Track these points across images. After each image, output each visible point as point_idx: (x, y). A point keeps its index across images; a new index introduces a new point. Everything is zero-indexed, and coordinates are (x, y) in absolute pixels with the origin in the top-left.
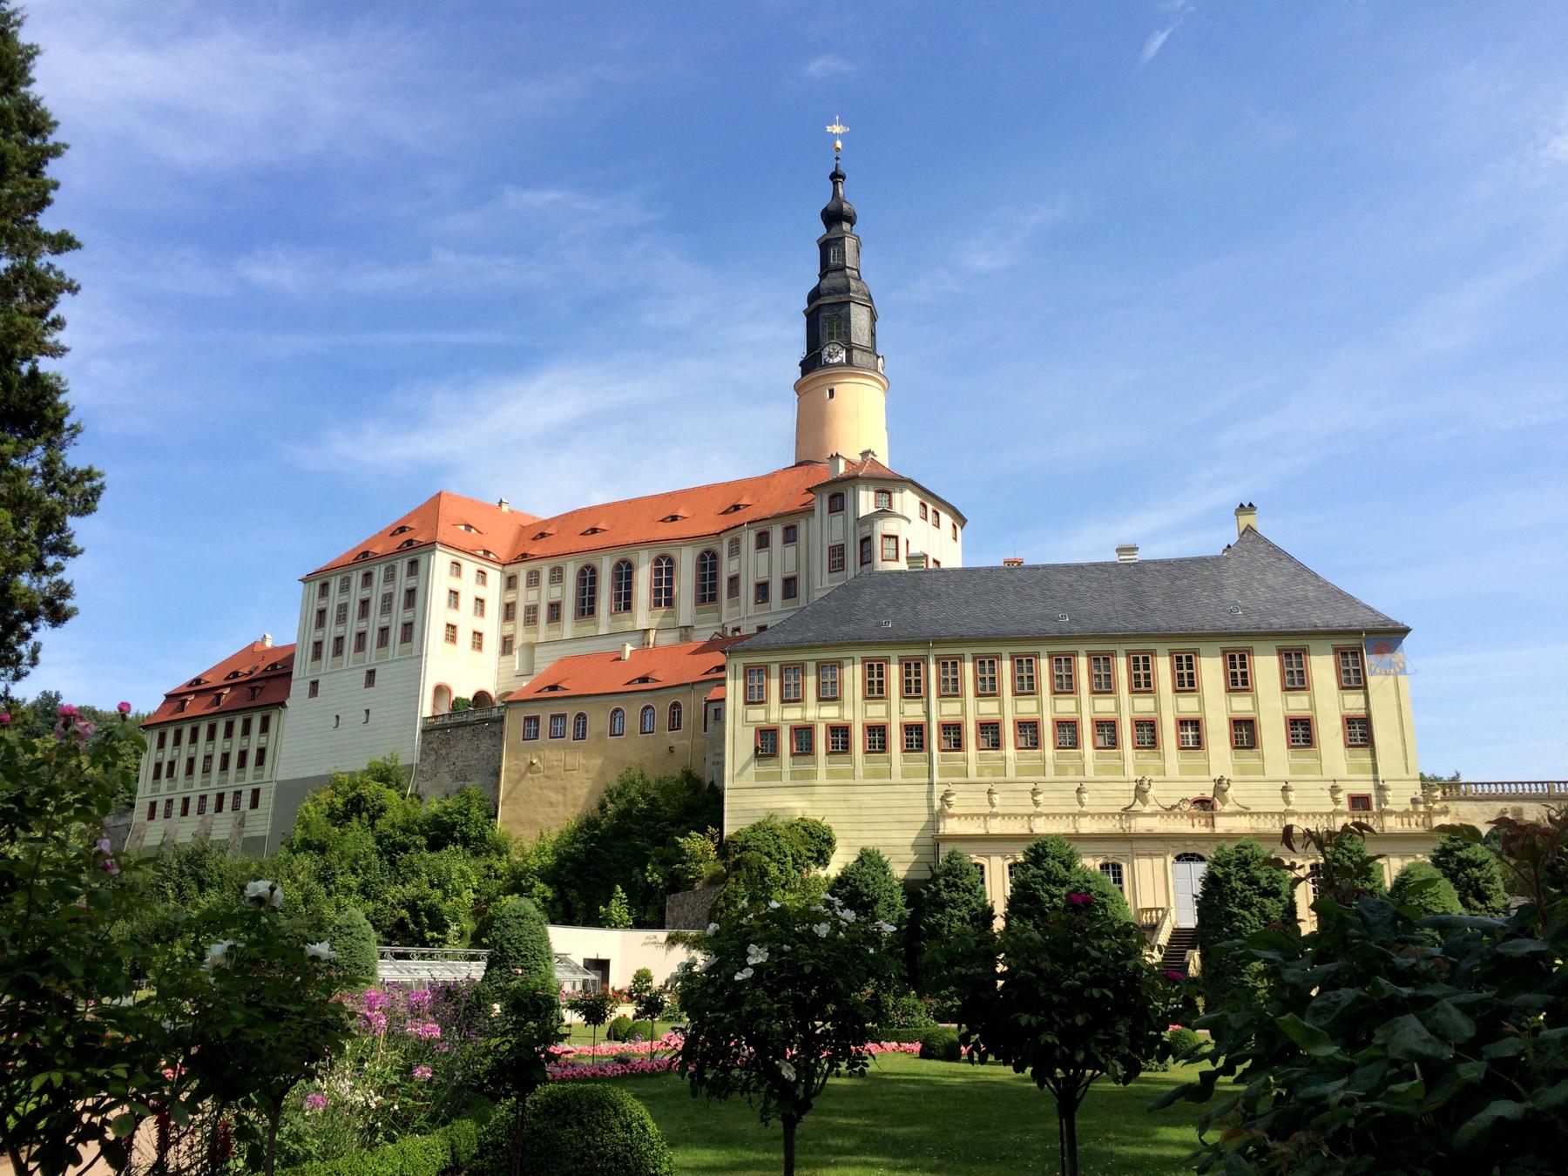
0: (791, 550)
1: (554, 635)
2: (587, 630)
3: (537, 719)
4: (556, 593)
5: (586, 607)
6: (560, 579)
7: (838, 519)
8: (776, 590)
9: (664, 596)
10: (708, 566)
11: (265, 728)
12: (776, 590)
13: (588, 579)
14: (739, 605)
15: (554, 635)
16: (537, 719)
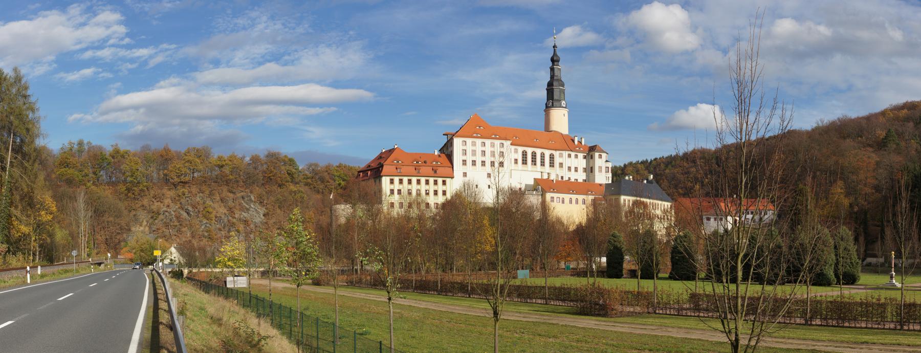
0: (576, 160)
1: (516, 168)
2: (524, 167)
3: (553, 198)
4: (516, 156)
5: (525, 162)
6: (517, 152)
7: (600, 160)
8: (573, 169)
9: (543, 164)
10: (552, 157)
11: (444, 183)
12: (573, 169)
13: (524, 154)
14: (563, 170)
15: (516, 168)
16: (553, 198)
